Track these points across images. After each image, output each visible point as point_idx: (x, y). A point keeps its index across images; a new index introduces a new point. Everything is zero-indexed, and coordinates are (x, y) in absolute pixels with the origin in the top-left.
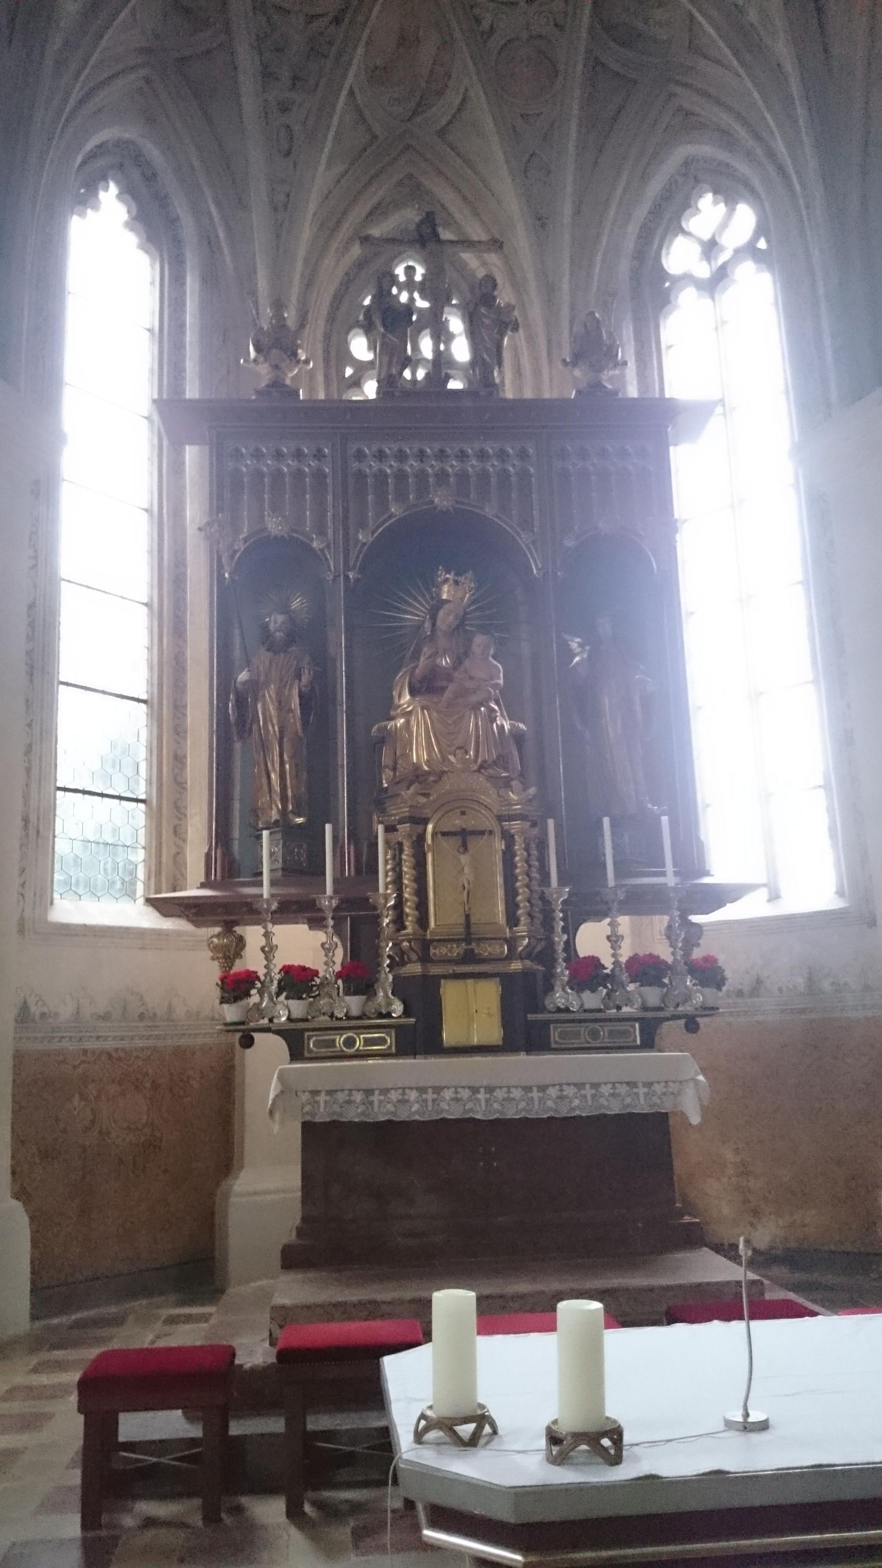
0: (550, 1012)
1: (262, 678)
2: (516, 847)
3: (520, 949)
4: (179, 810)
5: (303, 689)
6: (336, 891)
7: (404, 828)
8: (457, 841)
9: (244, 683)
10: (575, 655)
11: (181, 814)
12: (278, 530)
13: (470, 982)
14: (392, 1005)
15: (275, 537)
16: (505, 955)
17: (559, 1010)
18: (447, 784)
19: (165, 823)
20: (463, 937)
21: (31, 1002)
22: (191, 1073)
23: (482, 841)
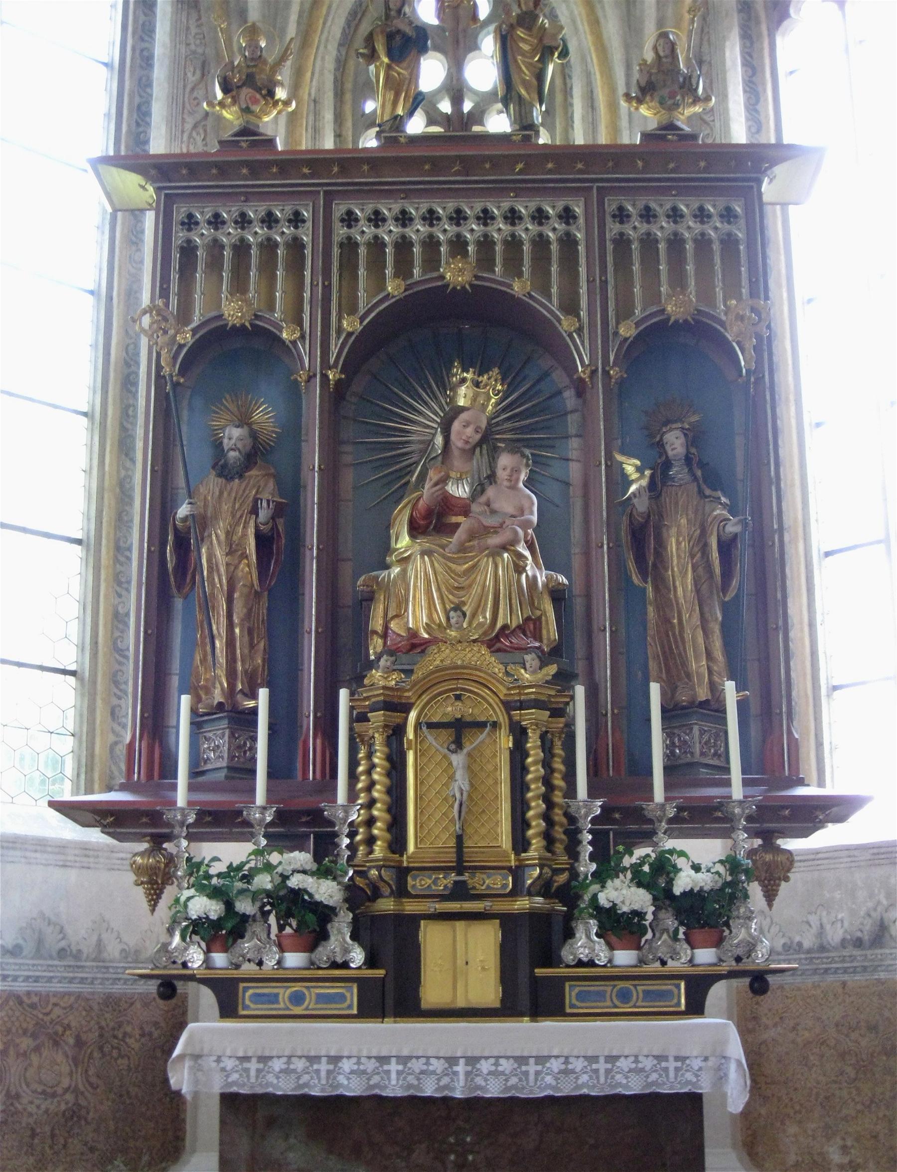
0: (568, 966)
2: (529, 745)
3: (529, 882)
5: (262, 527)
6: (270, 800)
7: (377, 718)
8: (446, 735)
9: (185, 519)
10: (633, 482)
11: (121, 690)
12: (237, 317)
13: (460, 925)
14: (350, 952)
15: (234, 326)
16: (508, 890)
17: (580, 964)
18: (437, 658)
19: (99, 703)
20: (454, 864)
22: (129, 1029)
23: (482, 737)
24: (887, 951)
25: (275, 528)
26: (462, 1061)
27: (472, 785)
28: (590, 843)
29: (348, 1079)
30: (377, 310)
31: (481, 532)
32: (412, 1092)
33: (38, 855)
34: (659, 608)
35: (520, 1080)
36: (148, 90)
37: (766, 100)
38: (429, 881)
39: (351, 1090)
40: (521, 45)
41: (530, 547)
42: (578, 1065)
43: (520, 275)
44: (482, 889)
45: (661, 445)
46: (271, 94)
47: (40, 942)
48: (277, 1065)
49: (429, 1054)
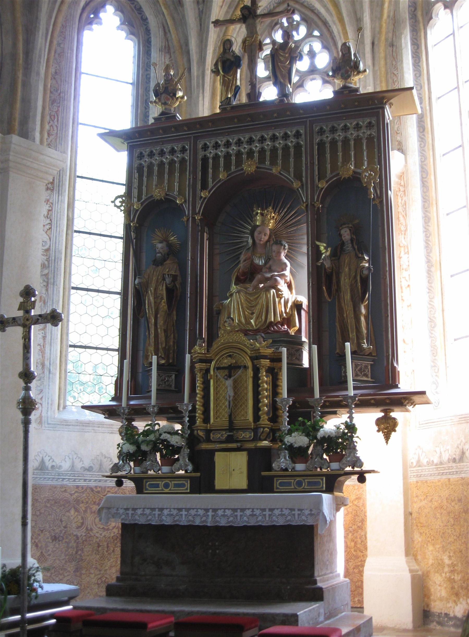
10: (323, 254)
15: (157, 199)
21: (46, 459)
24: (465, 464)
25: (175, 285)
26: (211, 510)
27: (235, 393)
28: (288, 417)
29: (166, 518)
30: (216, 186)
32: (190, 523)
33: (100, 429)
35: (234, 519)
37: (422, 60)
38: (219, 435)
39: (168, 522)
40: (281, 58)
42: (257, 512)
45: (340, 235)
46: (175, 95)
47: (101, 465)
48: (139, 512)
49: (198, 508)
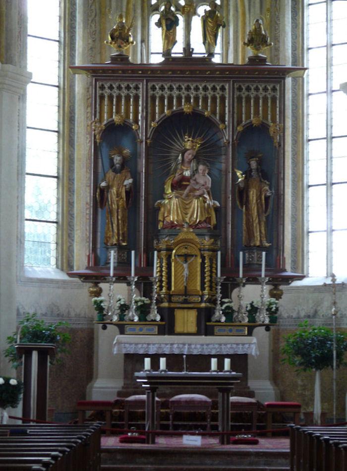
0: (214, 322)
1: (110, 184)
4: (70, 226)
10: (239, 178)
19: (65, 233)
21: (20, 307)
22: (77, 339)
24: (317, 319)
27: (189, 272)
31: (193, 190)
34: (246, 215)
36: (75, 6)
41: (209, 194)
43: (207, 109)
44: (192, 300)
45: (249, 164)
46: (128, 40)
